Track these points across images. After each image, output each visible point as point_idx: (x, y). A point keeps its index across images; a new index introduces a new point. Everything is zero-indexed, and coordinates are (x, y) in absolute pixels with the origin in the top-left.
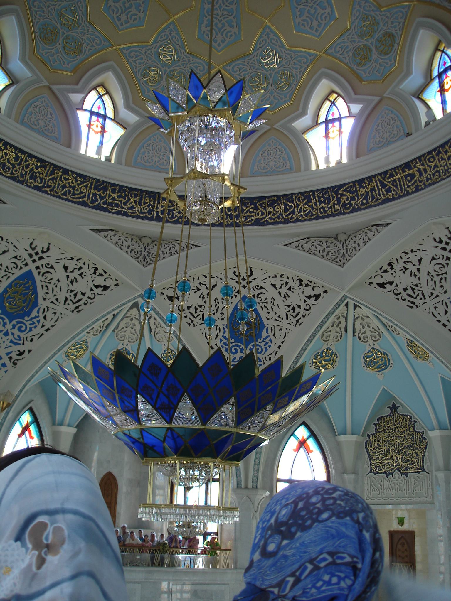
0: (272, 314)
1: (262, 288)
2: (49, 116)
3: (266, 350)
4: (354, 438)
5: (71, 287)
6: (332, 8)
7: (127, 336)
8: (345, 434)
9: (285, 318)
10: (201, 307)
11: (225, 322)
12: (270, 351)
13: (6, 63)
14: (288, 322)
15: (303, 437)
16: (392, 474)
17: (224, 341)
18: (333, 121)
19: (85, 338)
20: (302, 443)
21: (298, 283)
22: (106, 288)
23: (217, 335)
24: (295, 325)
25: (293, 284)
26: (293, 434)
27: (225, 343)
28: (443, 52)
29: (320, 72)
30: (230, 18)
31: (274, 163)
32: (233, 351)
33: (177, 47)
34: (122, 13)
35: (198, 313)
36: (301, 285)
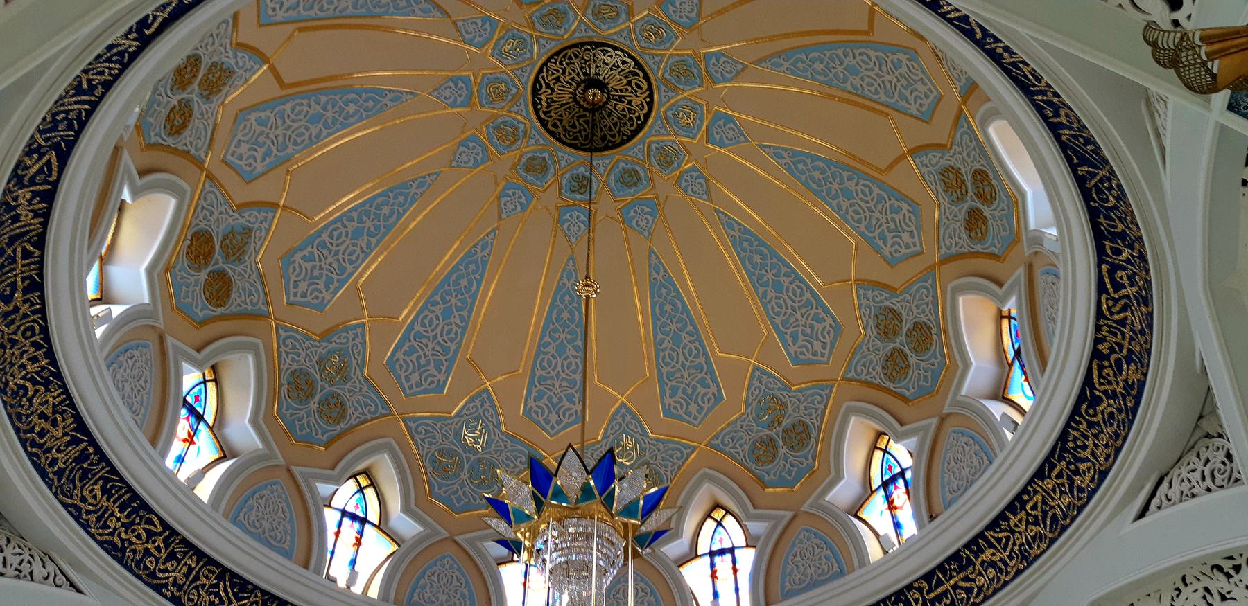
2: (455, 583)
6: (832, 316)
13: (387, 520)
18: (893, 479)
28: (1010, 317)
29: (843, 410)
30: (703, 374)
31: (813, 569)
33: (637, 436)
34: (550, 412)
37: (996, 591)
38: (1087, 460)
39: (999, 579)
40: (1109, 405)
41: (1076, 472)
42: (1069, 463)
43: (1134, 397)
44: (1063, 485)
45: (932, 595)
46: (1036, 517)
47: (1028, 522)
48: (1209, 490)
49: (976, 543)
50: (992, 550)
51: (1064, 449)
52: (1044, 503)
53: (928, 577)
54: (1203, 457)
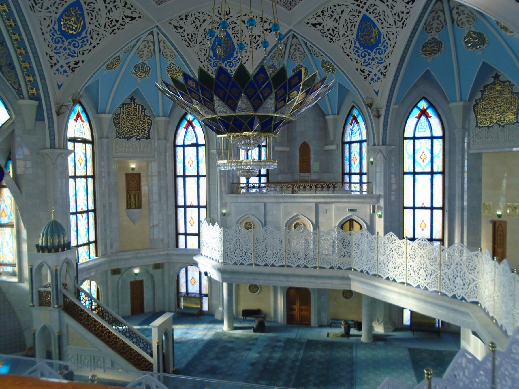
0: (385, 23)
1: (375, 5)
3: (385, 51)
4: (462, 103)
8: (456, 101)
9: (394, 24)
10: (336, 28)
11: (355, 36)
12: (388, 51)
14: (396, 26)
15: (424, 108)
17: (356, 49)
20: (423, 112)
23: (351, 47)
24: (402, 28)
26: (416, 106)
27: (356, 51)
32: (363, 55)
35: (335, 32)
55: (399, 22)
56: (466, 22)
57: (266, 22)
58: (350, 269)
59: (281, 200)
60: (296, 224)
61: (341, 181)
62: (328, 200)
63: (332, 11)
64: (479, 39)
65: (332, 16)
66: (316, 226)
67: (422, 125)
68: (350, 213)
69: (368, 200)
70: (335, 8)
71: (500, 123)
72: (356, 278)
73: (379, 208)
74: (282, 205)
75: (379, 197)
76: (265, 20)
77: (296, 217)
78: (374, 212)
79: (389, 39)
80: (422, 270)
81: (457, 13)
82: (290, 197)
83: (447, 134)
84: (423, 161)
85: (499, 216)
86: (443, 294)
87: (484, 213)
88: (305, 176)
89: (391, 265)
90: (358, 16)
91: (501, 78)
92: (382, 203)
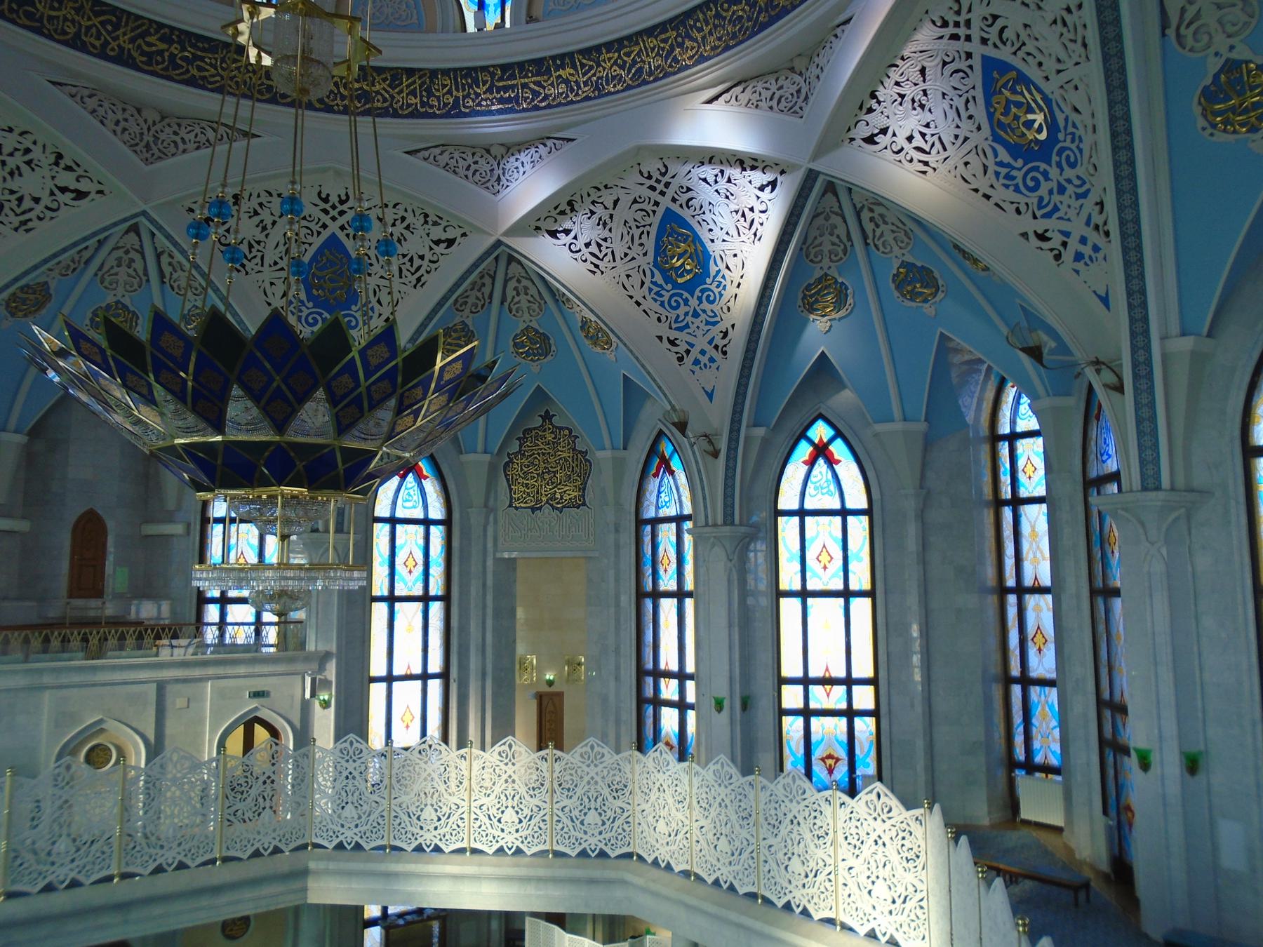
4: (487, 457)
5: (11, 184)
7: (121, 281)
10: (258, 243)
16: (540, 508)
19: (42, 279)
21: (422, 220)
22: (80, 195)
25: (414, 220)
35: (254, 252)
36: (426, 222)
37: (560, 104)
38: (696, 40)
39: (567, 96)
40: (743, 10)
41: (681, 45)
42: (679, 35)
43: (770, 16)
44: (663, 49)
45: (501, 84)
46: (625, 62)
47: (615, 63)
48: (771, 108)
49: (564, 59)
50: (572, 71)
51: (683, 23)
52: (638, 54)
53: (504, 67)
54: (780, 83)
55: (409, 274)
56: (525, 309)
57: (68, 168)
58: (305, 847)
59: (47, 679)
60: (92, 749)
61: (193, 619)
62: (197, 672)
63: (261, 205)
64: (538, 344)
65: (256, 213)
66: (155, 750)
67: (409, 494)
68: (254, 704)
69: (299, 667)
70: (270, 199)
71: (554, 503)
72: (332, 866)
73: (326, 684)
74: (47, 697)
75: (324, 658)
76: (70, 163)
77: (97, 729)
78: (313, 695)
79: (379, 302)
80: (510, 811)
81: (516, 289)
82: (81, 669)
83: (456, 516)
84: (410, 572)
85: (550, 683)
86: (558, 854)
87: (522, 679)
88: (91, 607)
89: (429, 814)
90: (319, 233)
91: (556, 421)
92: (331, 671)
